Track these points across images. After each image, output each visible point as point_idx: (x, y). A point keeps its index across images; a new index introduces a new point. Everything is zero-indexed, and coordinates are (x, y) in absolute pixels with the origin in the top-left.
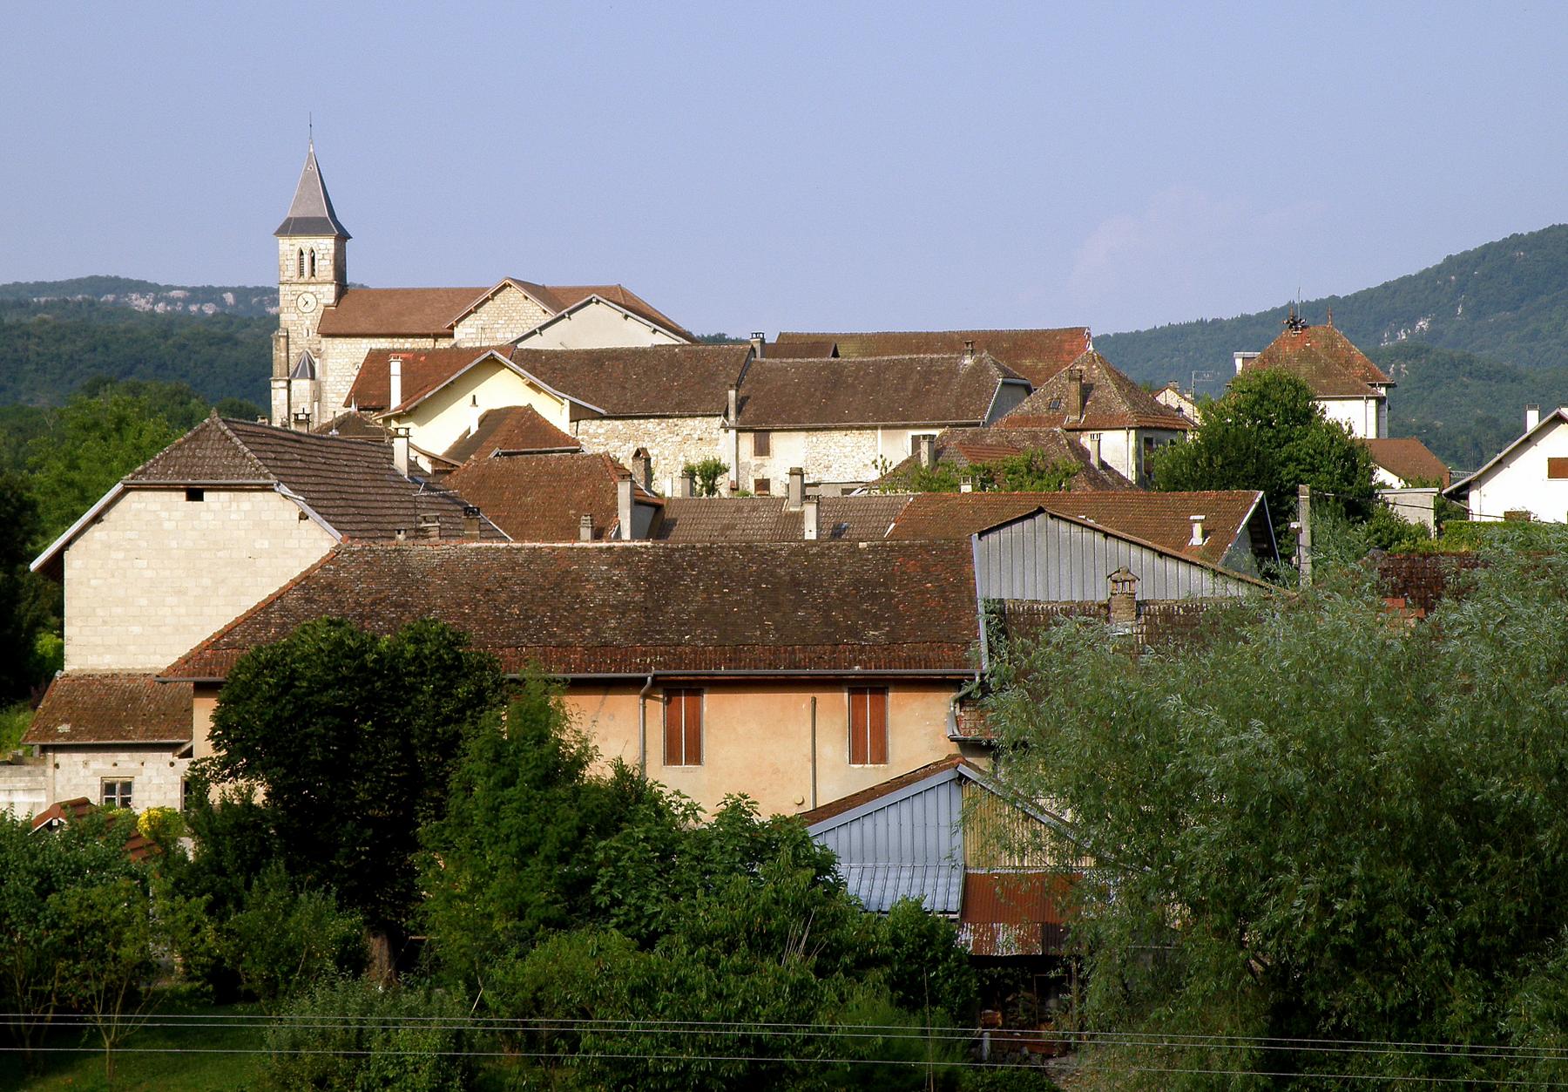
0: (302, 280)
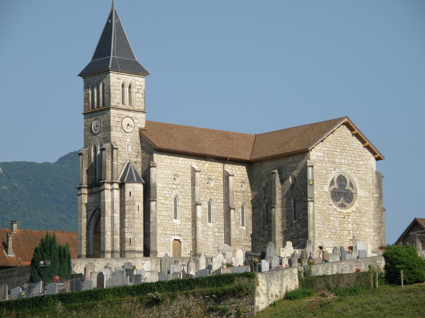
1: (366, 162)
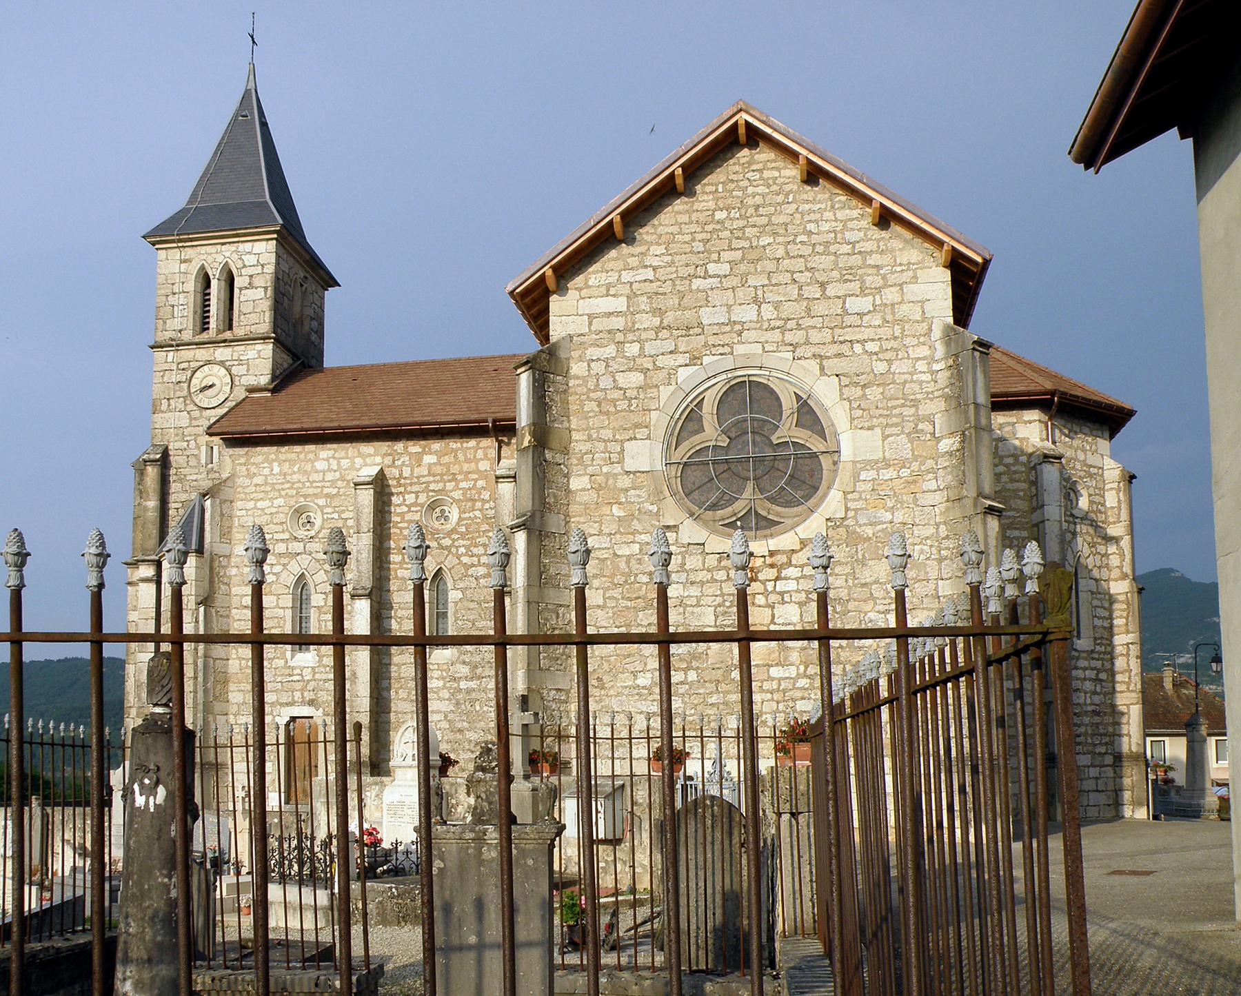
0: (205, 337)
1: (891, 295)
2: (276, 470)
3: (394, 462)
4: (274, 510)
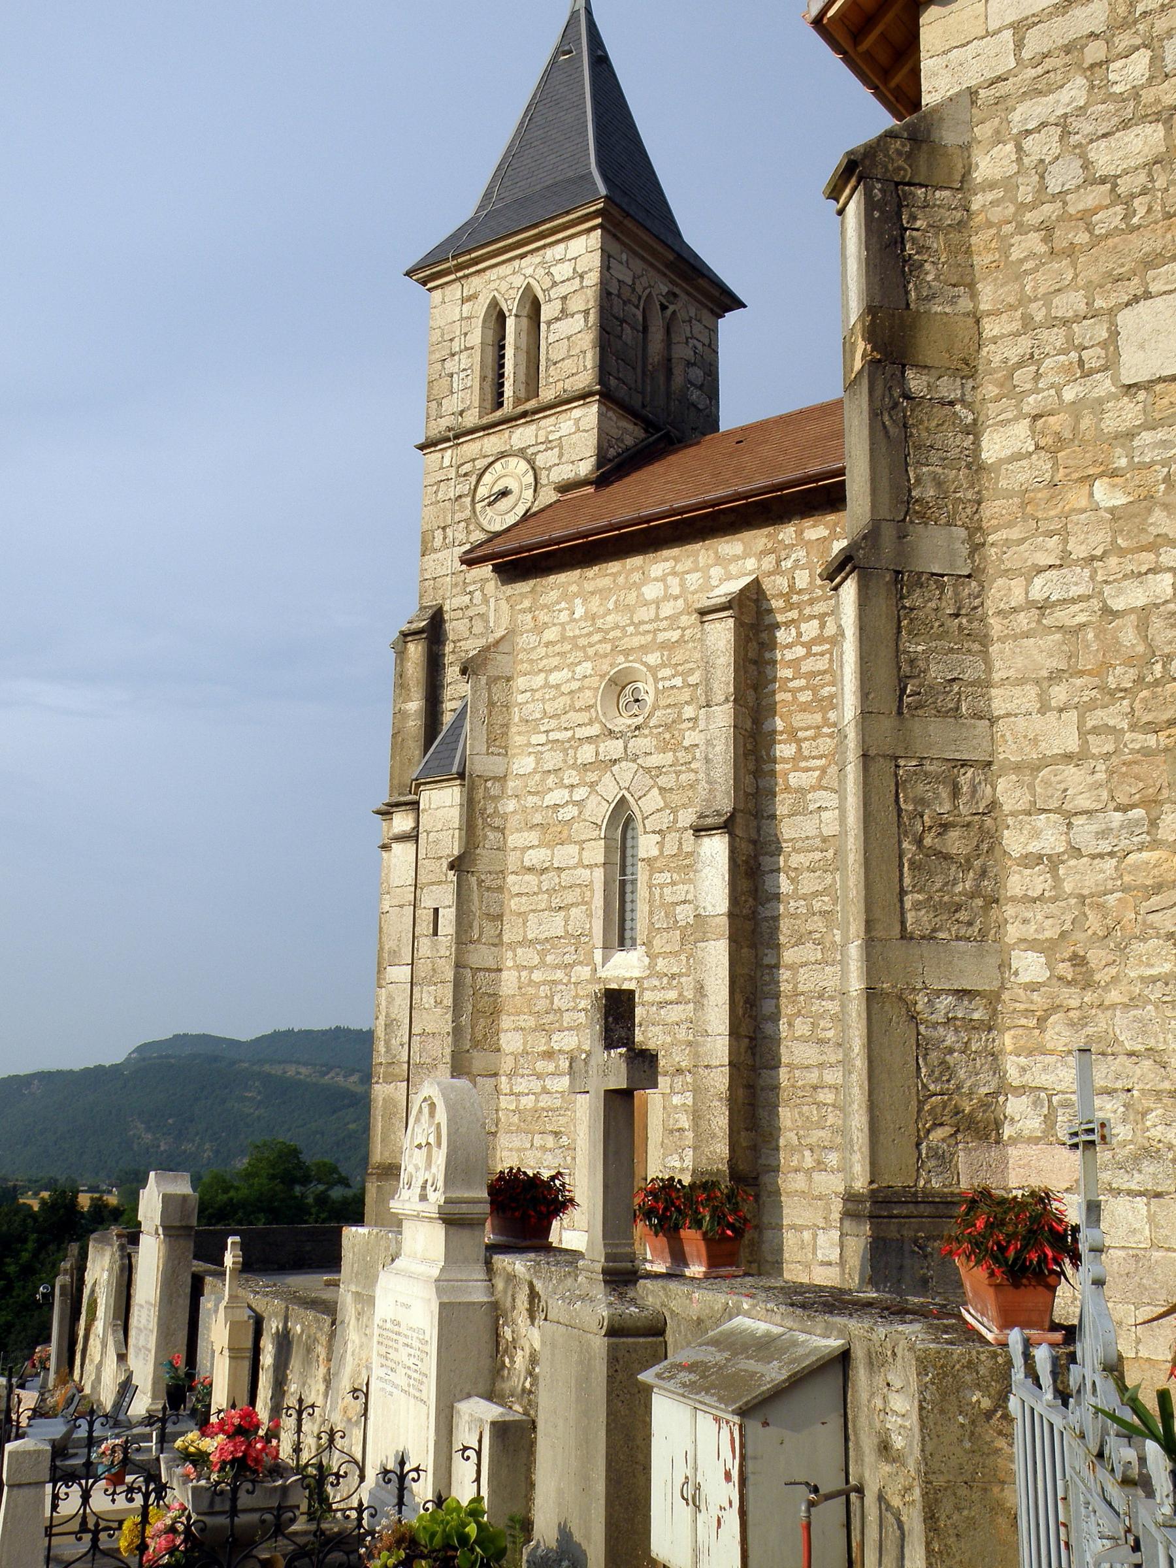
2: (579, 612)
3: (778, 562)
4: (575, 685)
